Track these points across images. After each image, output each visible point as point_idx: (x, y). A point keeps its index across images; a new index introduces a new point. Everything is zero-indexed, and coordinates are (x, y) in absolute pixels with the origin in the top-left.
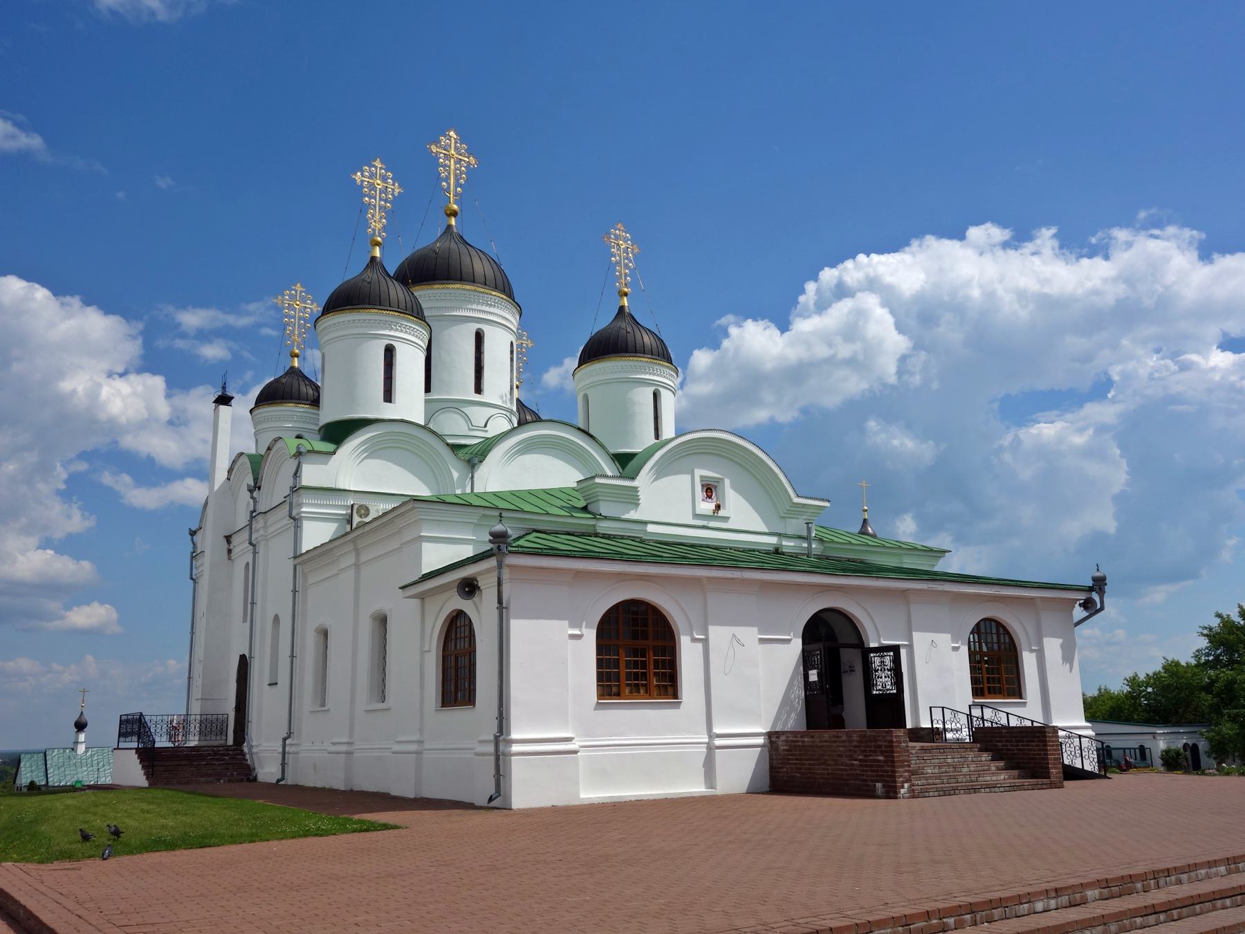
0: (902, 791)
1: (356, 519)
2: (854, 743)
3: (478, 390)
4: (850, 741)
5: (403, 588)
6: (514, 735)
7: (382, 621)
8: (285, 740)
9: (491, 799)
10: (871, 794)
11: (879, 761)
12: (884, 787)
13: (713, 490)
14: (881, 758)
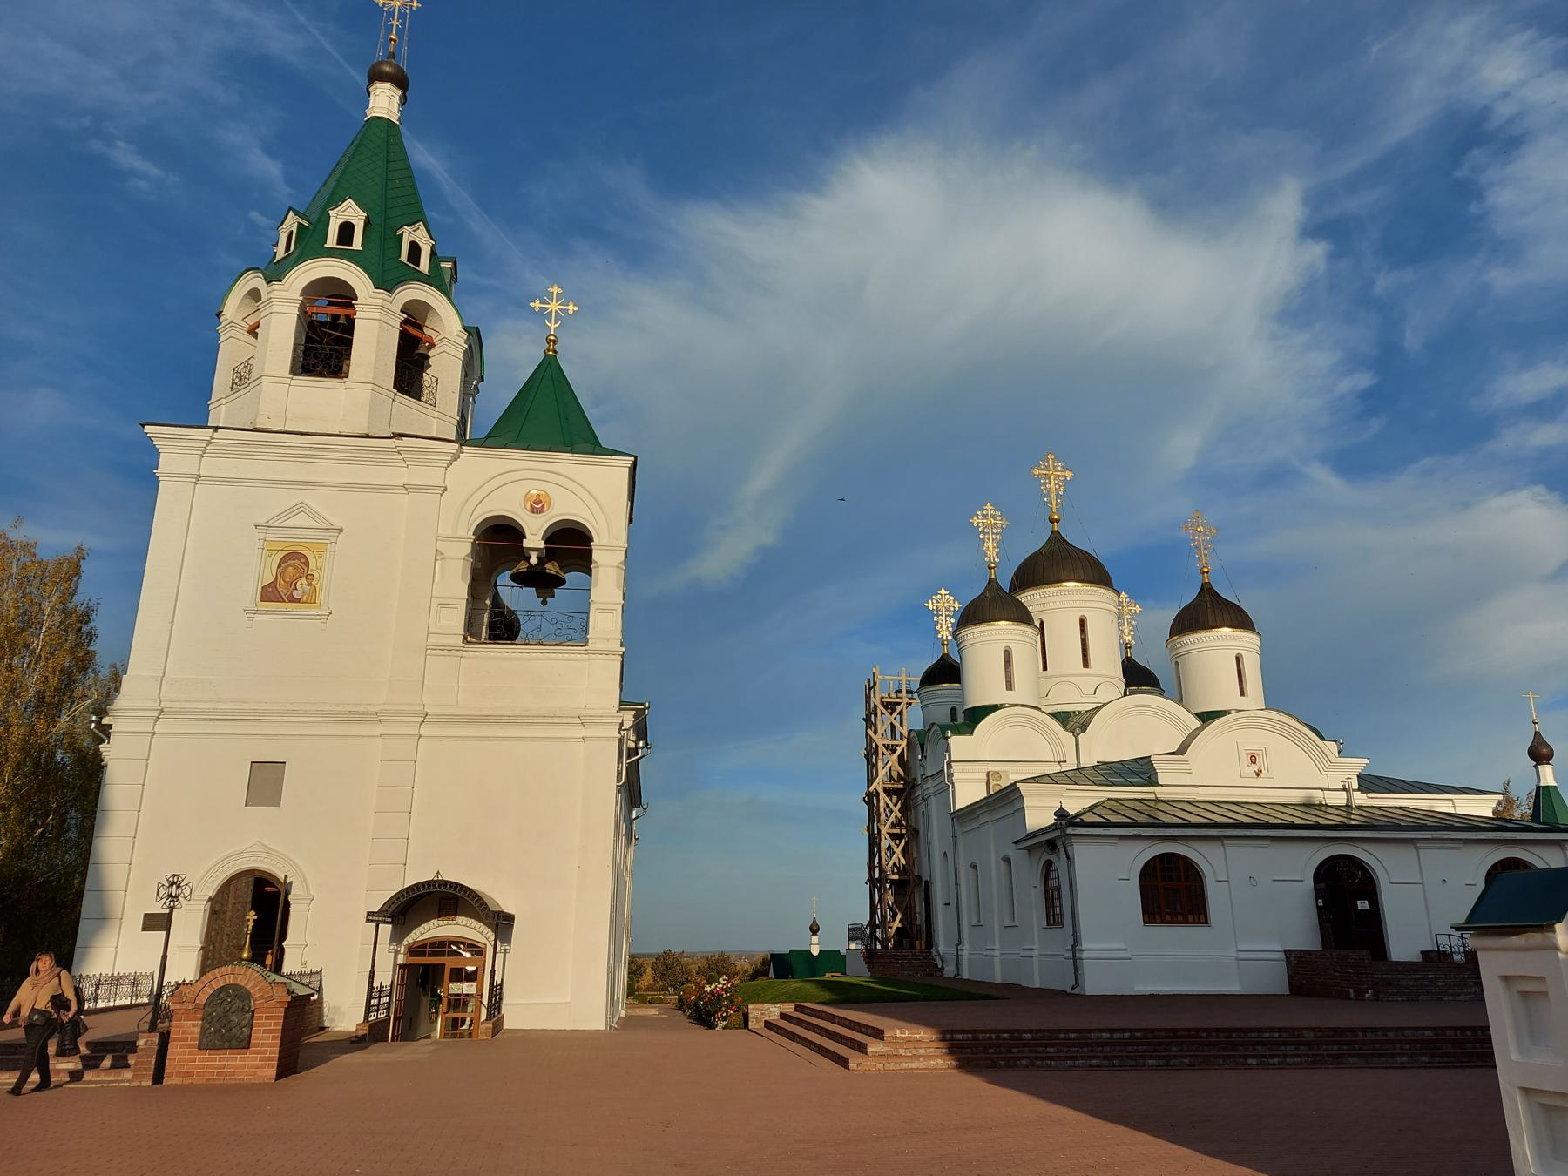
0: (1367, 995)
1: (992, 783)
2: (1335, 960)
3: (1086, 664)
4: (1333, 958)
5: (1015, 843)
6: (1084, 946)
7: (1008, 860)
8: (957, 946)
9: (1073, 988)
10: (1347, 997)
11: (1350, 973)
12: (1354, 991)
14: (1351, 971)
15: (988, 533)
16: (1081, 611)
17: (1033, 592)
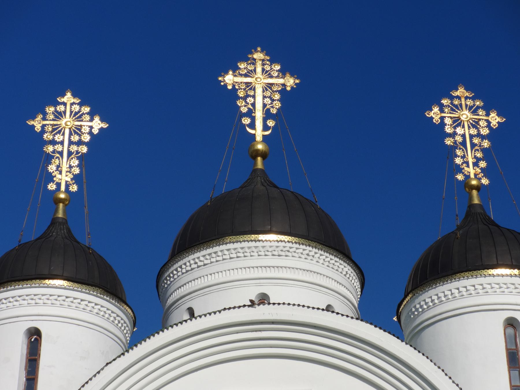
15: (62, 143)
17: (185, 261)
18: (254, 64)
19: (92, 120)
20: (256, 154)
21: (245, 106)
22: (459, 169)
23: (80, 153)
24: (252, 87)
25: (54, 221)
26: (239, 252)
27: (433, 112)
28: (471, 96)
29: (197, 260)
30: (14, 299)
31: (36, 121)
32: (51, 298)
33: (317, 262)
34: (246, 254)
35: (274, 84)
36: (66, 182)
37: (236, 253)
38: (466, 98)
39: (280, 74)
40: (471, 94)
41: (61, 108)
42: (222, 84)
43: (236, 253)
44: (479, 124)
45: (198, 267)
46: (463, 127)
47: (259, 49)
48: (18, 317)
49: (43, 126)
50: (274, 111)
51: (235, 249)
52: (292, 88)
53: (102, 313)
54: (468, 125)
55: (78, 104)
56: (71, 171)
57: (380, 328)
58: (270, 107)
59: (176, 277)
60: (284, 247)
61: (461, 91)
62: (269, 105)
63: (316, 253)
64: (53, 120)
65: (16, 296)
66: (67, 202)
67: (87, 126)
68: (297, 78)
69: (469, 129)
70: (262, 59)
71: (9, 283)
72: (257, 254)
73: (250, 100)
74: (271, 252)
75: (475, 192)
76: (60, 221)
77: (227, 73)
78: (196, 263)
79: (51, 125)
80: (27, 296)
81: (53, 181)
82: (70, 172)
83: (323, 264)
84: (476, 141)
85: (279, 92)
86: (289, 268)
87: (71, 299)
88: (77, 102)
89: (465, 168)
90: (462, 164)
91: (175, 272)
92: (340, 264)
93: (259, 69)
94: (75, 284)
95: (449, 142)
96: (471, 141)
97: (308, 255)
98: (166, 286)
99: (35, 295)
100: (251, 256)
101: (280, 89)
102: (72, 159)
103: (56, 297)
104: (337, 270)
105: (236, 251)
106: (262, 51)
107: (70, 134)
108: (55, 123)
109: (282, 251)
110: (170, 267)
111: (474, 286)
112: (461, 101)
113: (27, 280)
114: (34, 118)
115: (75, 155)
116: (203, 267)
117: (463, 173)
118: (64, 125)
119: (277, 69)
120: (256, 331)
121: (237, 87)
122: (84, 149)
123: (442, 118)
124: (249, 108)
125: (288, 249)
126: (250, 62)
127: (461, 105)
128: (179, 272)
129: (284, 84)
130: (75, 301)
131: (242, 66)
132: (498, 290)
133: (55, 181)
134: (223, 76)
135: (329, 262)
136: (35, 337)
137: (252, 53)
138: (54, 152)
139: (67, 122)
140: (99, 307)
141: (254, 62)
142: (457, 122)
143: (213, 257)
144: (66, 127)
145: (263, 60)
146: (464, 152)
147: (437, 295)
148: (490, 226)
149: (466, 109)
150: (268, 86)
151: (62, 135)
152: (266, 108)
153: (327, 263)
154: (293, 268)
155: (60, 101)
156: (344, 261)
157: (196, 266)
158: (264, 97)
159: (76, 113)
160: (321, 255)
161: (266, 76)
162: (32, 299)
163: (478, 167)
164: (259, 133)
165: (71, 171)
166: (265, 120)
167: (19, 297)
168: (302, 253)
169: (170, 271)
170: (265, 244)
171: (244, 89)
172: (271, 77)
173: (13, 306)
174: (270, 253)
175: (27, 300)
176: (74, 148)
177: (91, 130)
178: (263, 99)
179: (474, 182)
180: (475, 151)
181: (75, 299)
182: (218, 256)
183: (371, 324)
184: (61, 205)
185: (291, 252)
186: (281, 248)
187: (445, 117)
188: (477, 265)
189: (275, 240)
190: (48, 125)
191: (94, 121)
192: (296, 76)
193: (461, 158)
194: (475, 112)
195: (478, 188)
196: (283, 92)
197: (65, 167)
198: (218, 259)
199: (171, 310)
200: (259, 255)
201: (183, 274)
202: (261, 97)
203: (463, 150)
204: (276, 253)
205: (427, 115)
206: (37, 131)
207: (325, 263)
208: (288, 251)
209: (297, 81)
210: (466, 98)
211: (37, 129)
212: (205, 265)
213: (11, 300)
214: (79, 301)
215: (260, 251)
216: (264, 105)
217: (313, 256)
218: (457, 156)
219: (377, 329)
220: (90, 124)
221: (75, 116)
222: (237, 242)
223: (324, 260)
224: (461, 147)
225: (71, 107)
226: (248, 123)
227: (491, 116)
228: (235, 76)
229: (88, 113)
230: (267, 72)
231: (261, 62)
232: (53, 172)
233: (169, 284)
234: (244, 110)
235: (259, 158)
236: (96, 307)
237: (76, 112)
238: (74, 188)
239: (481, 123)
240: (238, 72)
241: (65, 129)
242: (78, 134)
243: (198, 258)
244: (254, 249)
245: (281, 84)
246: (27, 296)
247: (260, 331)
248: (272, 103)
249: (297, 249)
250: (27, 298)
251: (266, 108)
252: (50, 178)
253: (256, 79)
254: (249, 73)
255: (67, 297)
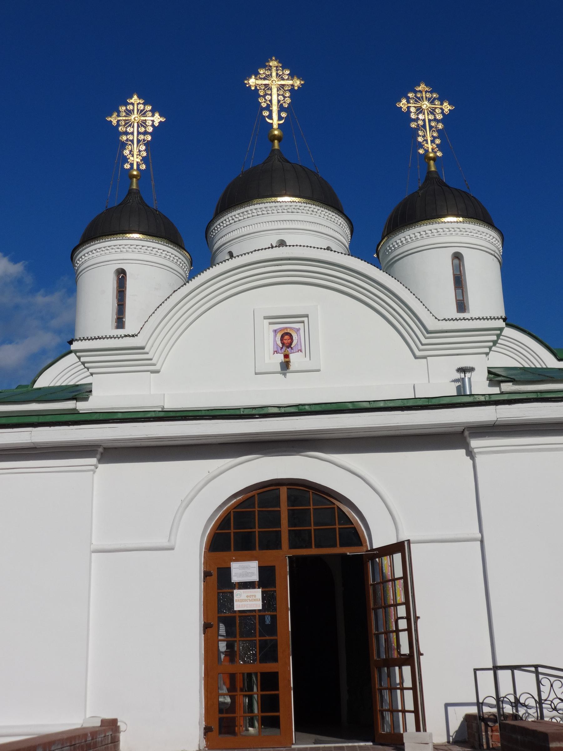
13: (295, 336)
15: (132, 133)
16: (277, 234)
17: (225, 217)
18: (270, 70)
19: (153, 116)
20: (274, 137)
21: (265, 102)
22: (420, 145)
23: (146, 141)
24: (269, 88)
25: (131, 192)
26: (263, 211)
27: (402, 103)
28: (429, 90)
29: (234, 217)
30: (105, 248)
31: (113, 118)
32: (131, 247)
33: (319, 216)
34: (268, 212)
35: (285, 85)
36: (137, 162)
37: (261, 211)
38: (426, 92)
39: (290, 77)
40: (430, 89)
41: (130, 107)
42: (247, 86)
43: (261, 211)
44: (435, 112)
45: (235, 222)
46: (424, 114)
47: (274, 58)
48: (109, 261)
49: (118, 121)
50: (286, 106)
51: (260, 208)
52: (299, 87)
53: (168, 257)
54: (428, 112)
55: (143, 104)
56: (140, 154)
57: (365, 261)
58: (283, 102)
59: (219, 229)
60: (296, 206)
61: (422, 87)
62: (282, 101)
63: (318, 210)
64: (125, 116)
65: (106, 247)
66: (139, 177)
67: (150, 120)
68: (302, 80)
69: (428, 116)
70: (276, 66)
71: (101, 238)
72: (276, 211)
73: (268, 97)
74: (286, 210)
75: (432, 162)
76: (135, 191)
77: (250, 77)
78: (233, 219)
79: (124, 120)
80: (114, 246)
81: (128, 162)
82: (140, 155)
83: (323, 217)
84: (433, 124)
85: (289, 90)
86: (300, 221)
87: (146, 248)
88: (142, 102)
89: (425, 144)
90: (423, 142)
91: (218, 226)
92: (336, 217)
93: (274, 74)
94: (148, 236)
95: (413, 125)
96: (429, 124)
97: (313, 211)
98: (212, 236)
99: (120, 245)
100: (272, 213)
101: (290, 88)
102: (141, 145)
103: (135, 246)
104: (334, 222)
105: (261, 210)
106: (276, 60)
107: (138, 127)
108: (127, 118)
109: (294, 209)
110: (215, 223)
111: (431, 230)
112: (422, 94)
113: (114, 234)
114: (111, 115)
115: (143, 142)
116: (238, 222)
117: (423, 148)
118: (133, 120)
119: (287, 73)
120: (278, 266)
121: (258, 88)
122: (149, 138)
123: (409, 108)
124: (267, 104)
125: (298, 207)
126: (267, 68)
127: (422, 97)
128: (221, 226)
129: (293, 85)
130: (148, 249)
131: (261, 72)
132: (448, 233)
133: (129, 162)
134: (248, 79)
135: (328, 216)
136: (122, 275)
137: (268, 62)
138: (127, 140)
139: (135, 117)
140: (166, 252)
141: (270, 68)
142: (420, 110)
143: (245, 214)
144: (135, 121)
145: (277, 67)
146: (424, 133)
147: (405, 237)
148: (442, 187)
149: (426, 100)
150: (281, 87)
151: (132, 128)
152: (280, 104)
153: (326, 217)
154: (302, 221)
155: (129, 102)
156: (339, 215)
157: (233, 221)
158: (278, 95)
159: (142, 111)
160: (322, 211)
161: (279, 79)
162: (118, 248)
163: (435, 143)
164: (275, 122)
165: (140, 154)
166: (279, 112)
167: (109, 247)
168: (308, 210)
169: (215, 225)
170: (282, 204)
171: (264, 89)
172: (283, 79)
173: (105, 253)
174: (285, 211)
175: (115, 249)
176: (141, 137)
177: (153, 123)
178: (278, 96)
179: (431, 155)
180: (432, 132)
181: (148, 247)
182: (249, 214)
183: (358, 258)
184: (135, 179)
185: (301, 210)
186: (294, 207)
187: (410, 107)
188: (433, 215)
189: (289, 201)
190: (122, 120)
191: (155, 117)
192: (301, 78)
193: (422, 137)
194: (432, 103)
195: (435, 159)
196: (292, 91)
197: (135, 152)
198: (249, 216)
199: (217, 252)
200: (278, 213)
201: (224, 227)
202: (276, 95)
203: (424, 131)
204: (290, 210)
205: (398, 106)
206: (114, 126)
207: (325, 217)
208: (299, 209)
209: (302, 82)
210: (426, 92)
211: (114, 123)
212: (239, 220)
213: (104, 249)
214: (151, 248)
215: (279, 209)
216: (279, 101)
217: (316, 212)
218: (419, 136)
219: (363, 261)
220: (152, 119)
221: (141, 112)
222: (262, 203)
223: (324, 214)
224: (422, 129)
225: (137, 106)
226: (267, 115)
227: (444, 105)
228: (257, 79)
229: (150, 111)
230: (280, 75)
231: (275, 68)
232: (127, 155)
233: (215, 235)
234: (264, 105)
235: (276, 141)
236: (163, 252)
237: (141, 110)
238: (143, 167)
239: (437, 111)
240: (258, 76)
241: (134, 123)
242: (144, 127)
243: (235, 216)
244: (274, 208)
245: (291, 85)
246: (114, 246)
247: (281, 265)
248: (284, 100)
249: (305, 207)
250: (114, 247)
251: (280, 104)
252: (125, 160)
253: (272, 81)
254: (267, 77)
255: (143, 246)
